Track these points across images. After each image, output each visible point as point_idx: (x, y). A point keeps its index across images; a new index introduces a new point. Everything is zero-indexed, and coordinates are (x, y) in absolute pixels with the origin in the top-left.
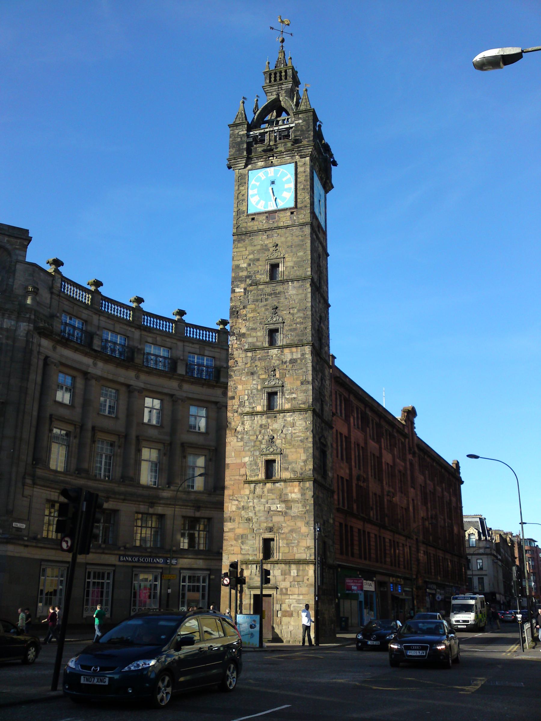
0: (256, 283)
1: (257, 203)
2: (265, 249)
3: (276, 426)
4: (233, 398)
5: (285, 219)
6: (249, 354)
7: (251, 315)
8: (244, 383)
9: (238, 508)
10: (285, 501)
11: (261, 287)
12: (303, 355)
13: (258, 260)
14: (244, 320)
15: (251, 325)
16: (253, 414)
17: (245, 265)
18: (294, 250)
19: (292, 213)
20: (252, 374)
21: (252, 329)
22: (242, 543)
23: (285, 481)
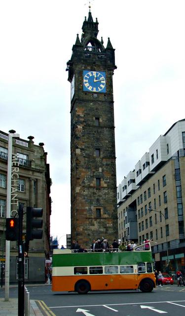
0: (89, 126)
1: (88, 87)
2: (91, 109)
3: (100, 193)
4: (79, 179)
5: (102, 98)
6: (87, 159)
7: (87, 140)
8: (84, 172)
9: (83, 230)
10: (106, 227)
11: (91, 128)
12: (112, 162)
13: (89, 114)
14: (84, 142)
15: (87, 145)
16: (89, 187)
17: (83, 116)
18: (106, 113)
19: (105, 95)
20: (89, 168)
21: (87, 147)
22: (86, 245)
23: (105, 219)
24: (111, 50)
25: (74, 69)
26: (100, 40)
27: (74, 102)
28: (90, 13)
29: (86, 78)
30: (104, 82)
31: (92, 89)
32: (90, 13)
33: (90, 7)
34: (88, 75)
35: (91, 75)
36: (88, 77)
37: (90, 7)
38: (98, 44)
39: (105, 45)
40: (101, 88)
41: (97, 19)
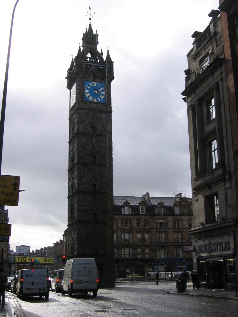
1: (89, 97)
24: (109, 63)
26: (100, 52)
27: (74, 111)
28: (90, 25)
29: (87, 89)
30: (104, 93)
31: (93, 99)
32: (90, 25)
33: (90, 19)
34: (89, 86)
35: (92, 86)
36: (89, 88)
37: (90, 19)
38: (97, 55)
39: (105, 57)
40: (100, 98)
41: (96, 31)
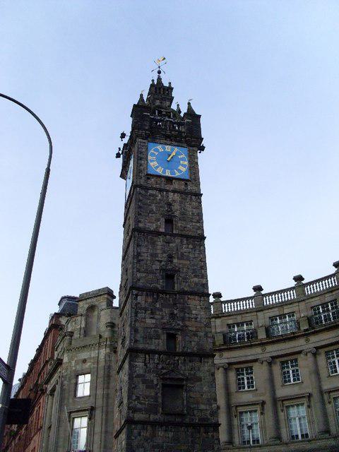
25: (131, 153)
28: (159, 79)
31: (164, 172)
33: (159, 72)
34: (157, 150)
37: (159, 72)
40: (181, 171)
41: (170, 83)
